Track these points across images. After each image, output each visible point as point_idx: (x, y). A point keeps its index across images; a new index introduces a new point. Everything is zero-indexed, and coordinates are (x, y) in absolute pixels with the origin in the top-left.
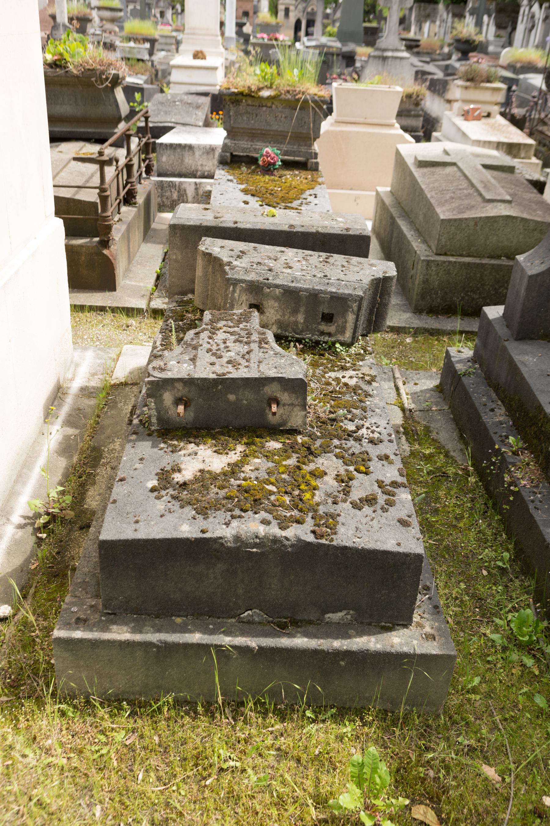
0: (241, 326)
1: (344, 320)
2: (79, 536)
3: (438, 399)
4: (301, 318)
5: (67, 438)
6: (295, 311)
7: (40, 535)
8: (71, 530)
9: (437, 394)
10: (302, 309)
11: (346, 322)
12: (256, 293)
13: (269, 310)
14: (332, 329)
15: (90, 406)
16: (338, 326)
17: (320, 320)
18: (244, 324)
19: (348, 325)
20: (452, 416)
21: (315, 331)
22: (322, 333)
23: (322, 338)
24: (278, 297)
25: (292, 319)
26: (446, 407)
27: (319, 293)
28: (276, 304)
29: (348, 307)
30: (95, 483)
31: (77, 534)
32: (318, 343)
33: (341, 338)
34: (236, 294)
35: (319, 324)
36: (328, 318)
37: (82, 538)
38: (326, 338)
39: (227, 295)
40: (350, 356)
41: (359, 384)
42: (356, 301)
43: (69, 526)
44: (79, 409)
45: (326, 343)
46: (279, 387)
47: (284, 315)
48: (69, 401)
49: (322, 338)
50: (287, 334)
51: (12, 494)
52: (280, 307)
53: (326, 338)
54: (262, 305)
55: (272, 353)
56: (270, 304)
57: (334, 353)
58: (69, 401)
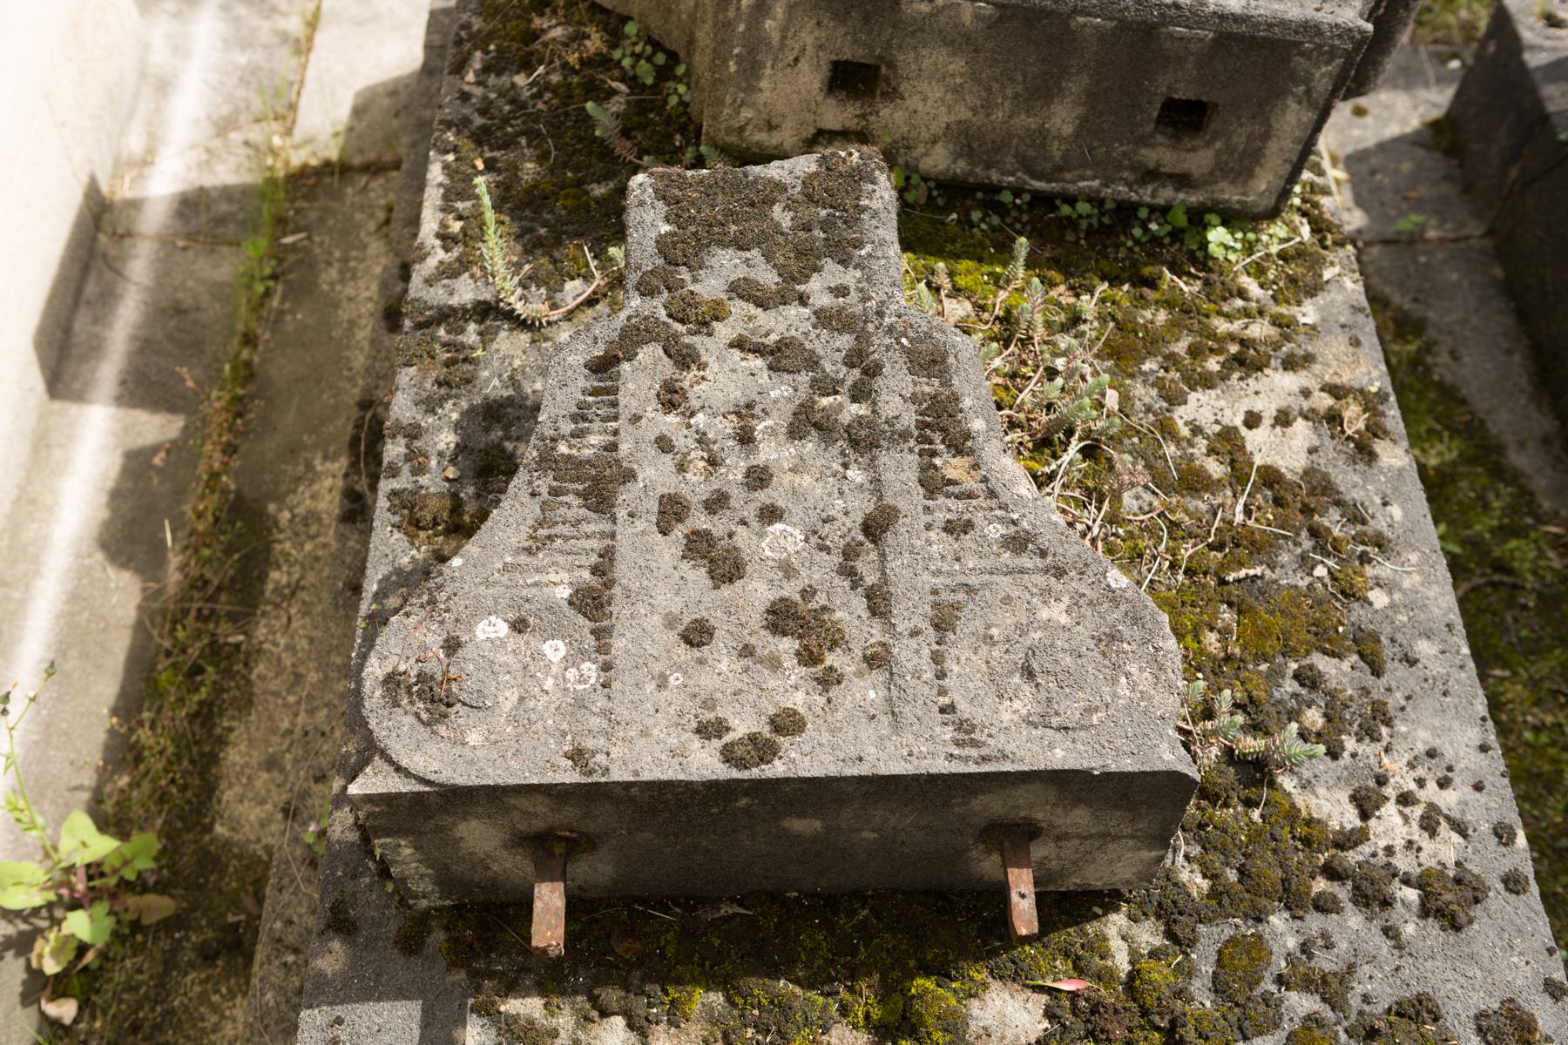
0: (816, 287)
1: (1258, 129)
2: (203, 998)
3: (1445, 188)
4: (1063, 118)
5: (136, 464)
6: (1042, 92)
7: (52, 1009)
8: (170, 962)
9: (1434, 162)
10: (1075, 85)
11: (1266, 136)
12: (866, 20)
13: (924, 86)
14: (1199, 160)
15: (220, 291)
16: (1229, 149)
17: (1149, 128)
18: (832, 273)
19: (1273, 146)
20: (1498, 272)
21: (1120, 167)
22: (1151, 175)
23: (1145, 194)
24: (967, 38)
25: (1026, 121)
26: (1474, 229)
27: (1165, 21)
28: (958, 65)
29: (1293, 78)
30: (250, 703)
31: (191, 982)
32: (1126, 213)
33: (1230, 194)
34: (769, 24)
35: (1145, 141)
36: (1186, 118)
37: (215, 1009)
38: (1166, 194)
39: (728, 25)
40: (1258, 271)
41: (1321, 461)
42: (1332, 54)
43: (165, 944)
44: (179, 311)
45: (1164, 211)
46: (1052, 796)
47: (988, 106)
48: (140, 267)
49: (1145, 194)
50: (995, 176)
51: (31, 502)
52: (974, 76)
53: (1166, 194)
54: (891, 65)
55: (996, 531)
56: (926, 63)
57: (1194, 260)
58: (140, 267)
